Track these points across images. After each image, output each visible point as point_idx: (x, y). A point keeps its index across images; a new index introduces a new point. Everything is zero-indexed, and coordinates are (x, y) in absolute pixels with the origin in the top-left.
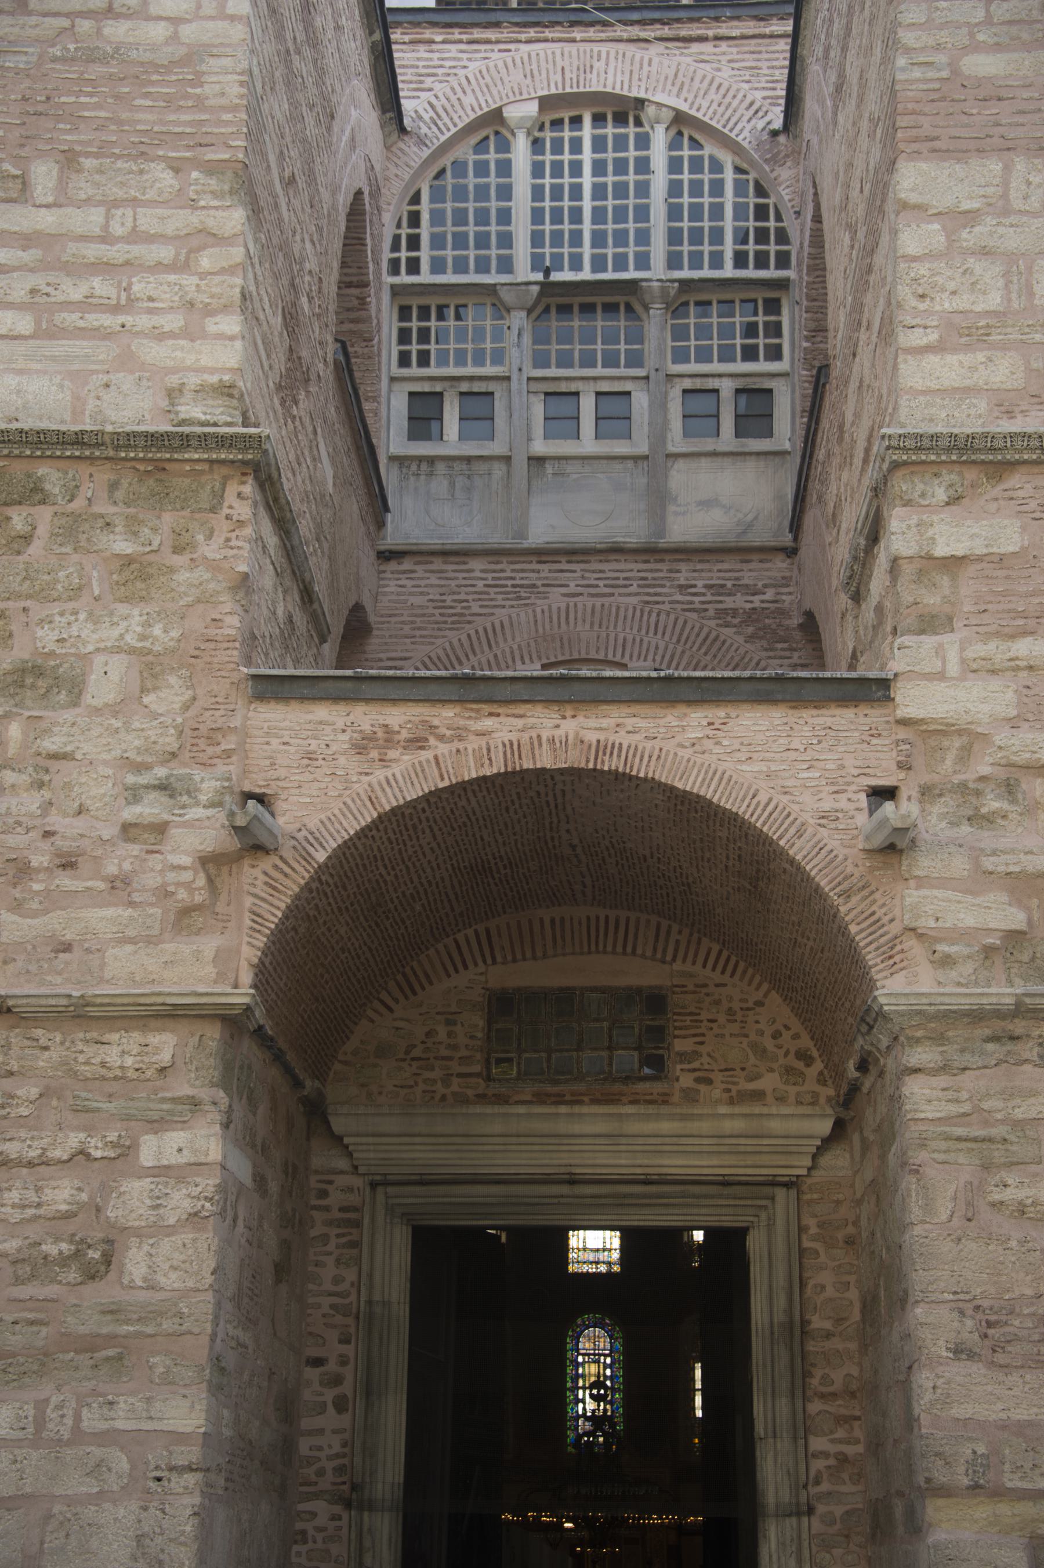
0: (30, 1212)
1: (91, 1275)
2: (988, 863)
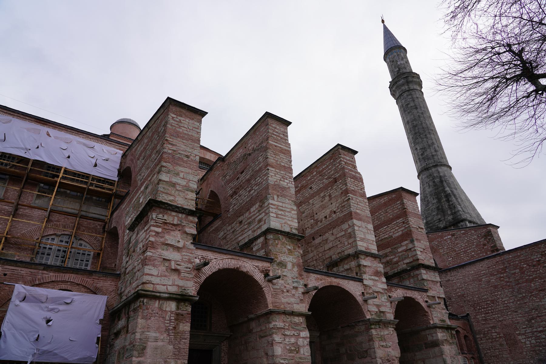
0: (289, 343)
1: (297, 353)
2: (374, 303)
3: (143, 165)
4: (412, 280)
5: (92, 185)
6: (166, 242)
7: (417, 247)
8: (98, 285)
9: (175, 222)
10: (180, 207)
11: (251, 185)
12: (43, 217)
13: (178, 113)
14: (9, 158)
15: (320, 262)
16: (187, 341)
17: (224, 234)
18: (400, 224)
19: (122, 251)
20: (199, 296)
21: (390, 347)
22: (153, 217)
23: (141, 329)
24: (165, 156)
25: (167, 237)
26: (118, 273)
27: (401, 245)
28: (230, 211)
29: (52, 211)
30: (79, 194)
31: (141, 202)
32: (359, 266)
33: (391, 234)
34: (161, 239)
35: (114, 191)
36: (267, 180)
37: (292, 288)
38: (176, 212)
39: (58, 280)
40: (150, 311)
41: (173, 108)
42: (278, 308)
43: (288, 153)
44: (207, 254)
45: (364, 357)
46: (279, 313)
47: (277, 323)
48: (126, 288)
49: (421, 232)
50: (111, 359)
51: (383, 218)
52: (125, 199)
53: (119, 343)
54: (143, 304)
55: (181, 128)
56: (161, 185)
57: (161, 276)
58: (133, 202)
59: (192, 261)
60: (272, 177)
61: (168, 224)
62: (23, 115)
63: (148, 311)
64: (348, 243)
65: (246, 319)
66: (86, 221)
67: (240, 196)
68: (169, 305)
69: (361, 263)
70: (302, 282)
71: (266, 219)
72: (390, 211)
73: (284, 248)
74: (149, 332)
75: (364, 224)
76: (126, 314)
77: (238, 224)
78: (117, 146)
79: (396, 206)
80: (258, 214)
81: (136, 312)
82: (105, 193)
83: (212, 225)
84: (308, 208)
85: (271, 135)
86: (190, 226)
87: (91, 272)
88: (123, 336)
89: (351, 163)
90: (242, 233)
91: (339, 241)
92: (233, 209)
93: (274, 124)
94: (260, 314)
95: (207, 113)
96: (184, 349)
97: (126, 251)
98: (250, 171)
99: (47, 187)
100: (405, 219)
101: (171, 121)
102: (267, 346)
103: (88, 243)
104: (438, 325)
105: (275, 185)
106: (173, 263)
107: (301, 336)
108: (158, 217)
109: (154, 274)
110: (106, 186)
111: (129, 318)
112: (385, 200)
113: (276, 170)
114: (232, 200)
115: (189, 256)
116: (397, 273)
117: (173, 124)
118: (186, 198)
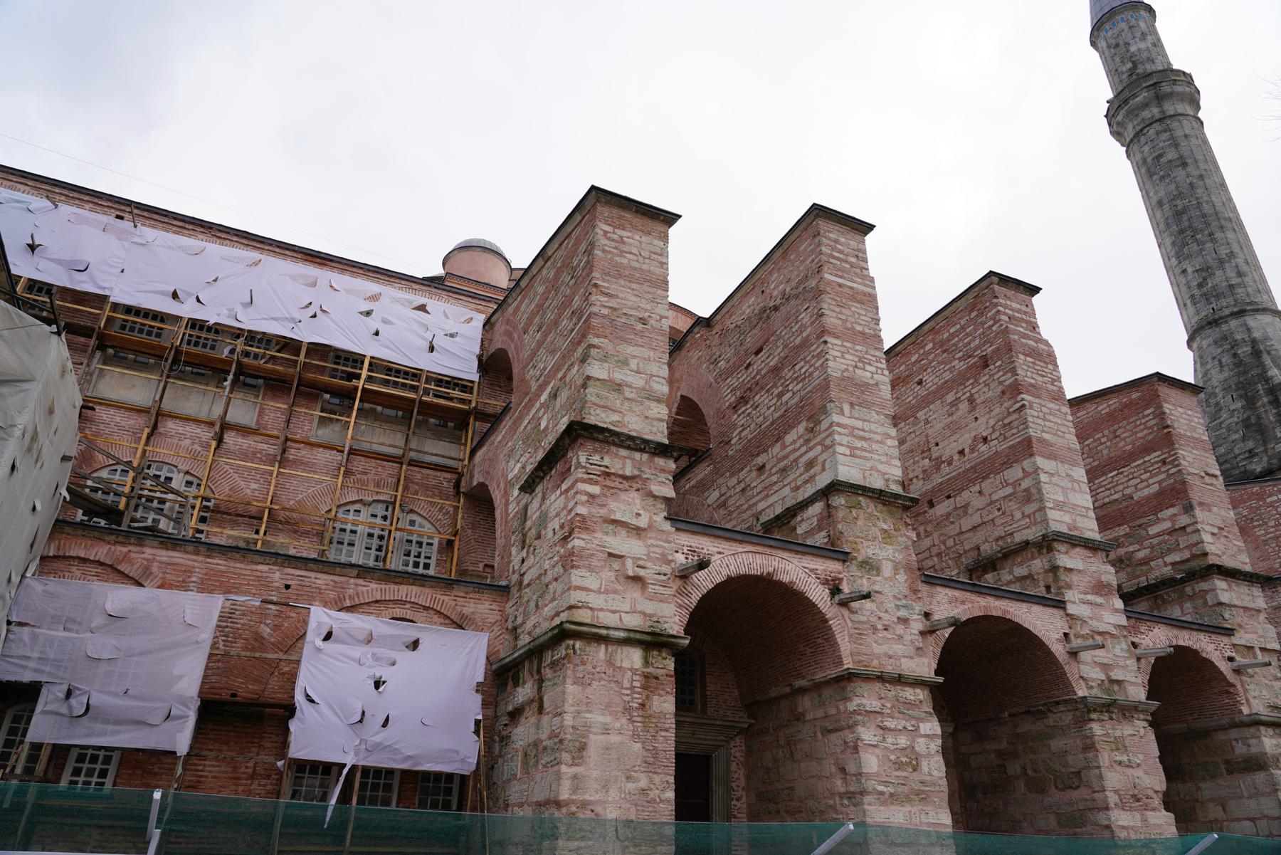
0: (895, 747)
1: (915, 770)
2: (1095, 659)
3: (540, 344)
4: (1188, 605)
5: (426, 392)
6: (612, 517)
7: (1202, 522)
8: (466, 611)
9: (628, 472)
10: (637, 438)
11: (783, 381)
12: (335, 464)
13: (615, 220)
14: (260, 341)
15: (950, 559)
16: (669, 734)
17: (721, 495)
18: (1152, 465)
19: (507, 538)
20: (690, 637)
21: (1139, 765)
22: (581, 460)
23: (573, 706)
24: (595, 322)
25: (613, 505)
26: (503, 583)
27: (1158, 518)
28: (733, 442)
29: (352, 452)
30: (400, 413)
31: (542, 427)
32: (1054, 569)
33: (1127, 492)
34: (600, 511)
35: (473, 404)
36: (824, 367)
37: (896, 620)
38: (628, 448)
39: (387, 599)
40: (589, 668)
41: (604, 211)
42: (866, 666)
43: (869, 300)
44: (700, 542)
45: (1071, 787)
46: (867, 678)
47: (864, 701)
48: (526, 616)
49: (1212, 485)
50: (505, 768)
51: (1106, 452)
52: (502, 421)
53: (522, 734)
54: (575, 653)
55: (625, 257)
56: (591, 389)
57: (607, 592)
58: (522, 428)
59: (670, 558)
60: (835, 360)
61: (613, 477)
62: (279, 247)
63: (584, 667)
64: (1023, 513)
65: (788, 690)
66: (418, 472)
67: (757, 407)
68: (627, 656)
69: (1060, 563)
70: (918, 607)
71: (825, 461)
72: (1125, 435)
73: (873, 528)
74: (590, 712)
75: (1063, 468)
76: (535, 673)
77: (754, 474)
78: (470, 304)
79: (1143, 421)
80: (804, 449)
81: (558, 668)
82: (454, 409)
83: (690, 476)
84: (914, 432)
85: (826, 259)
86: (659, 480)
87: (449, 582)
88: (533, 720)
89: (1024, 317)
90: (765, 493)
91: (999, 510)
92: (740, 439)
93: (832, 232)
94: (822, 680)
95: (680, 216)
96: (665, 751)
97: (517, 536)
98: (777, 347)
99: (337, 401)
100: (1169, 452)
101: (603, 241)
102: (843, 752)
103: (425, 518)
104: (1263, 718)
105: (843, 379)
106: (629, 563)
107: (923, 732)
108: (591, 461)
109: (591, 587)
110: (456, 393)
111: (543, 681)
112: (1112, 408)
113: (845, 344)
114: (736, 416)
115: (662, 547)
116: (1146, 588)
117: (606, 248)
118: (647, 417)
